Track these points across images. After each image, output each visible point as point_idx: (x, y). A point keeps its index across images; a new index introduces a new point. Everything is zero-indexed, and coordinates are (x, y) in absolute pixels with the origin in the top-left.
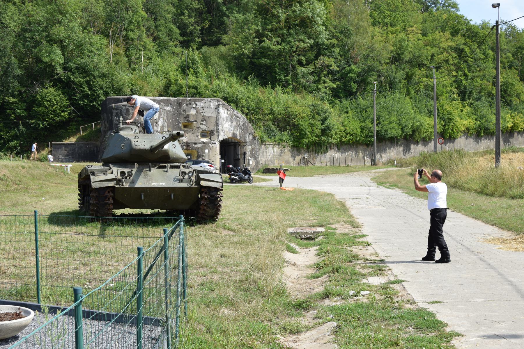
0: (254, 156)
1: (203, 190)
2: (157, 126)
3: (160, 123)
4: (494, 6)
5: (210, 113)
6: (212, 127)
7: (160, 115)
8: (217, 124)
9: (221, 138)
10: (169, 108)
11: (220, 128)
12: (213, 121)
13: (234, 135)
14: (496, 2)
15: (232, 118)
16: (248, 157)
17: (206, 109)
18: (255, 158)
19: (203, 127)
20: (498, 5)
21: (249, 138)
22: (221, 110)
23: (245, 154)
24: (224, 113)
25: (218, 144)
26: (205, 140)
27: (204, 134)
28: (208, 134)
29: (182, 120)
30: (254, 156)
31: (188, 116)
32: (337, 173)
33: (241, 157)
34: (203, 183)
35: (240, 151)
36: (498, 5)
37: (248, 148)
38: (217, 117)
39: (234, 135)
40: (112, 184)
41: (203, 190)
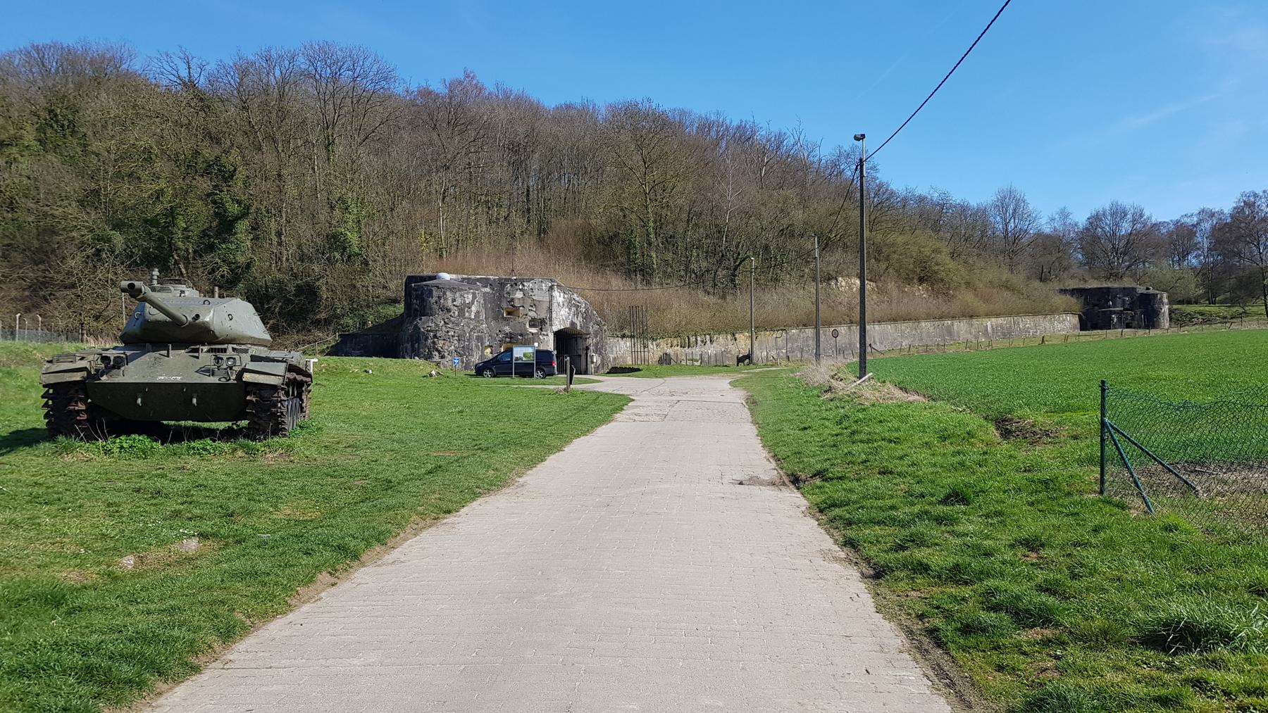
0: (598, 350)
1: (249, 389)
2: (470, 312)
3: (474, 308)
4: (856, 138)
5: (540, 296)
6: (543, 315)
7: (474, 297)
8: (550, 310)
9: (555, 329)
10: (488, 290)
11: (554, 316)
12: (546, 306)
13: (573, 324)
14: (859, 133)
15: (570, 304)
16: (591, 353)
17: (536, 292)
18: (600, 354)
19: (532, 314)
20: (863, 136)
21: (592, 328)
22: (556, 293)
23: (587, 348)
24: (559, 297)
25: (551, 336)
26: (534, 330)
27: (533, 323)
28: (540, 323)
29: (504, 305)
30: (598, 350)
31: (512, 300)
32: (712, 373)
33: (583, 353)
34: (247, 377)
35: (581, 345)
36: (863, 136)
37: (591, 341)
38: (551, 301)
39: (573, 324)
40: (78, 377)
41: (249, 389)
